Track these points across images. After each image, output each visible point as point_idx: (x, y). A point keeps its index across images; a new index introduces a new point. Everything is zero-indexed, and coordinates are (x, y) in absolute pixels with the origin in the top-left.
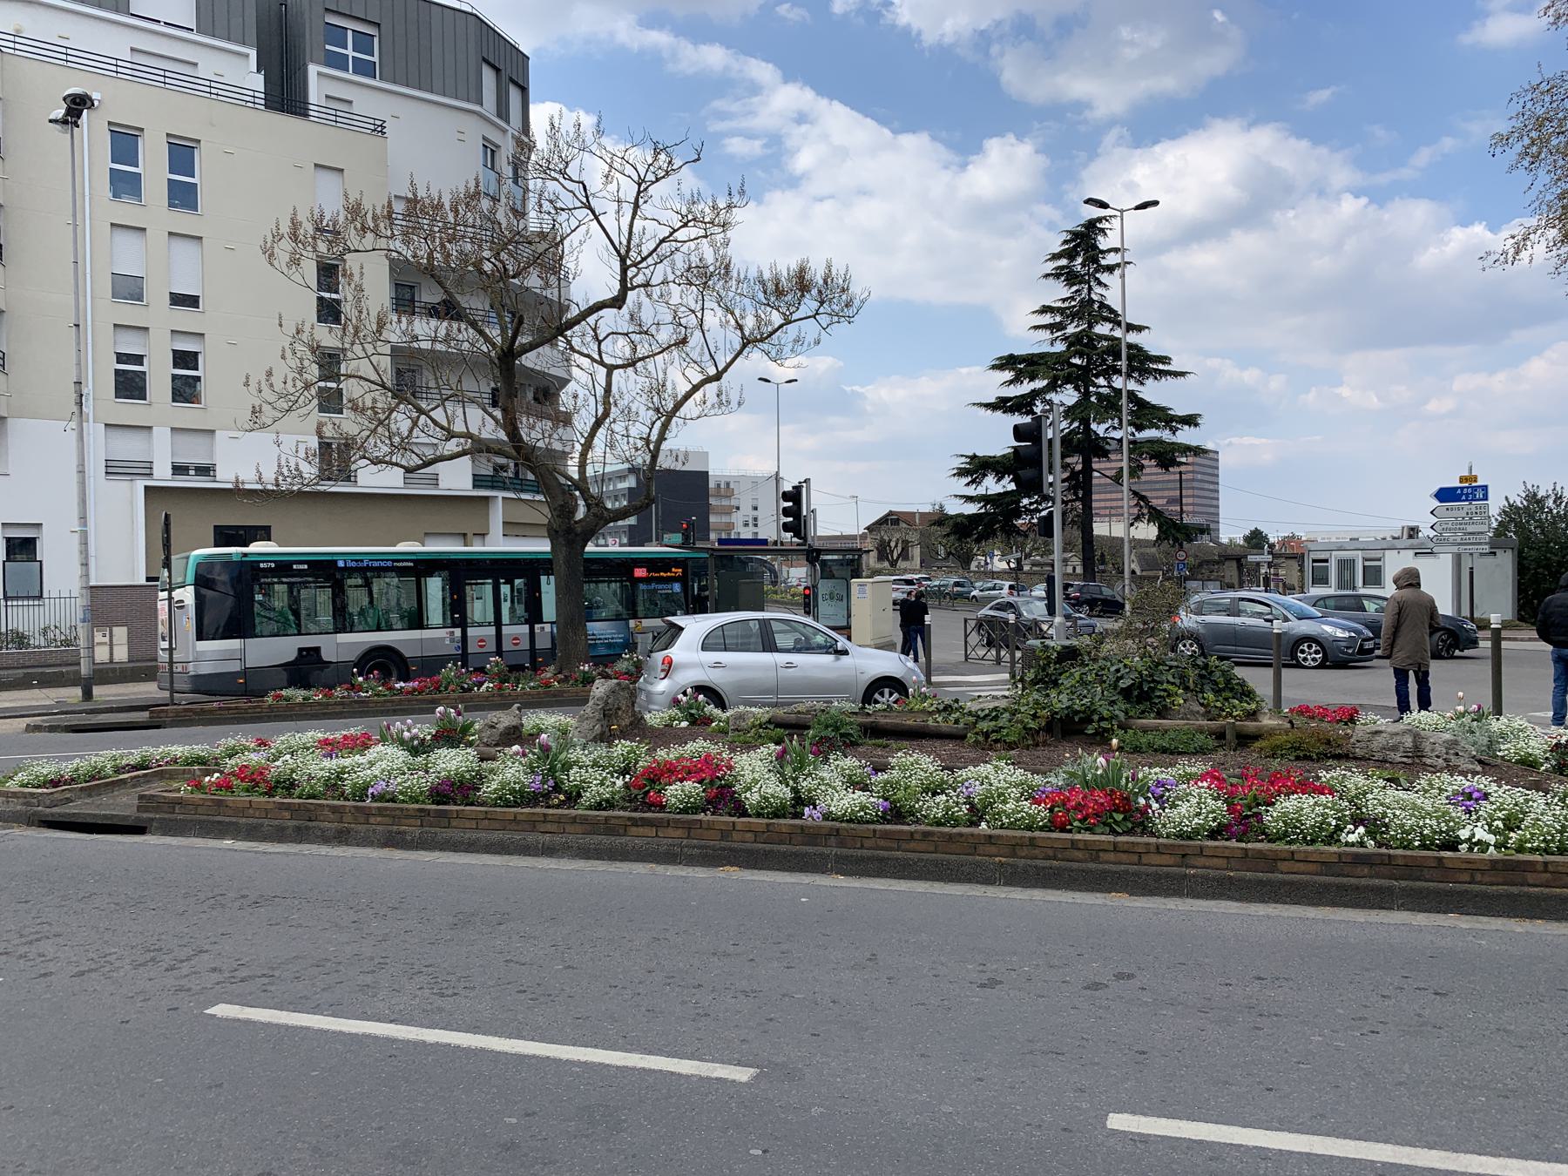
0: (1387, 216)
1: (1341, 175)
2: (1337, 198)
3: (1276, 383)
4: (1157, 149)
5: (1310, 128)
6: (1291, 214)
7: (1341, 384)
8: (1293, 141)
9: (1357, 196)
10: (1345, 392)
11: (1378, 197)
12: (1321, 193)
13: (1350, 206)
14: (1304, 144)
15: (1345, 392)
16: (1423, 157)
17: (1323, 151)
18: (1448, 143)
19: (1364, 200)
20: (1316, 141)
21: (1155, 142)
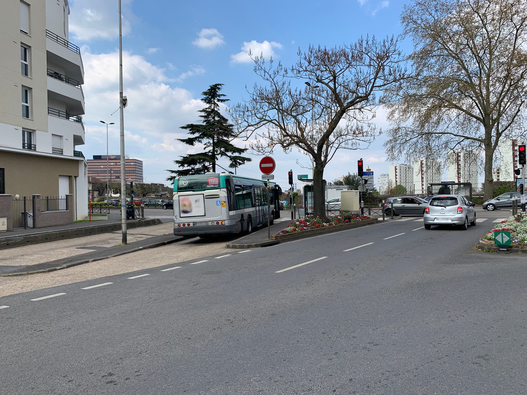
0: (174, 93)
1: (161, 77)
2: (160, 84)
3: (144, 140)
4: (100, 56)
5: (149, 59)
6: (146, 86)
7: (163, 143)
8: (145, 62)
9: (166, 85)
10: (164, 145)
11: (173, 86)
12: (155, 81)
13: (164, 88)
14: (149, 65)
15: (164, 145)
16: (183, 76)
17: (155, 68)
18: (190, 73)
19: (168, 86)
20: (153, 64)
21: (100, 54)
